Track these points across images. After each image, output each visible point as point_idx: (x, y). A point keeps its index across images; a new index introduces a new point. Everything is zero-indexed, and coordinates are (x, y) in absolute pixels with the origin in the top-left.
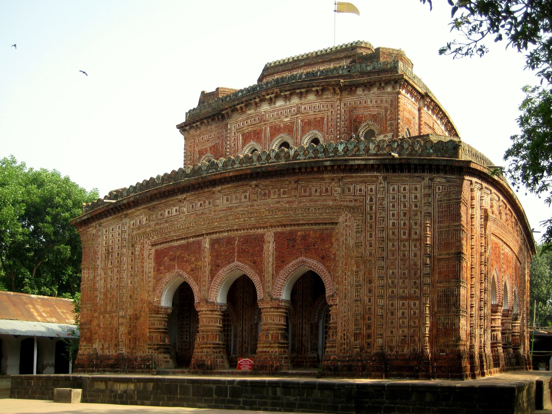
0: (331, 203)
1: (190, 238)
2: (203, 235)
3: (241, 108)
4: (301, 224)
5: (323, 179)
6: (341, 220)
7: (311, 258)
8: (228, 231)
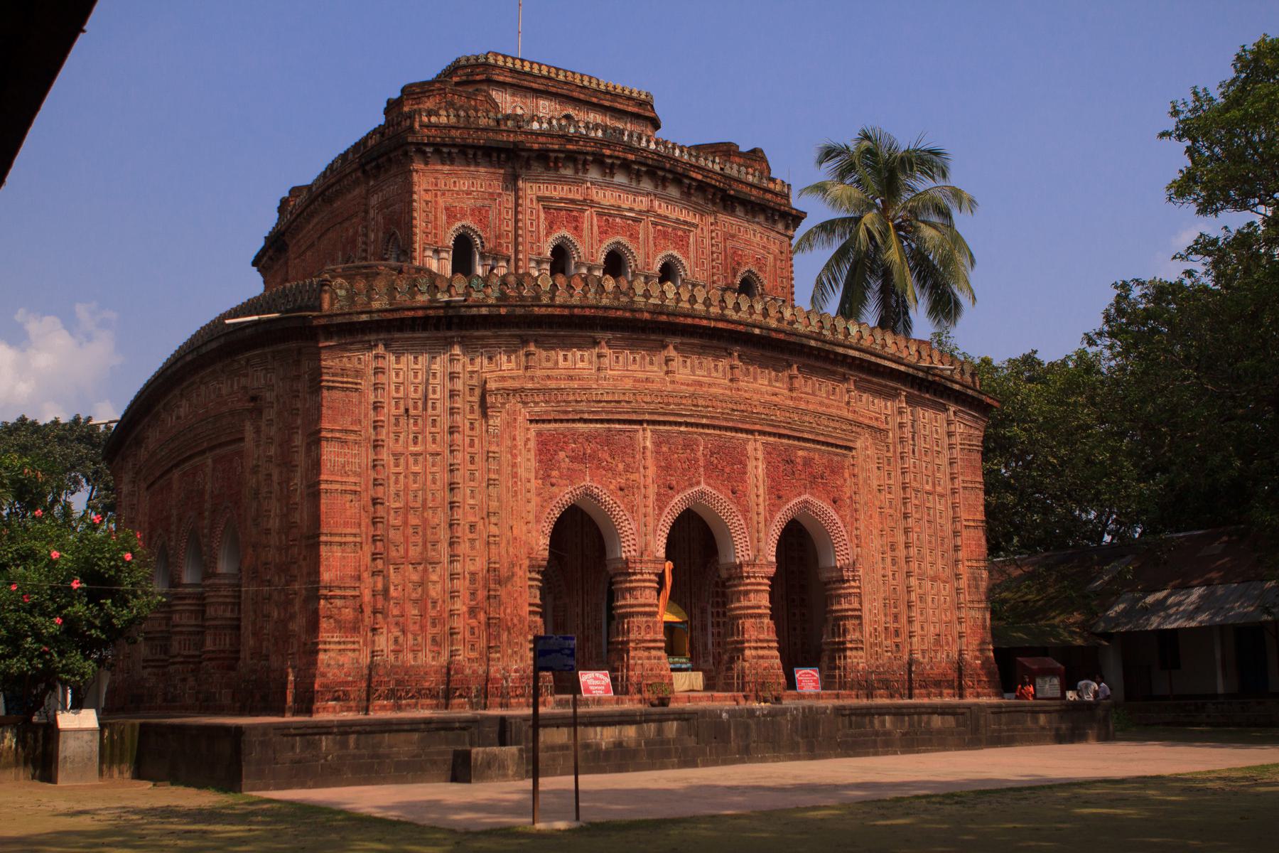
0: (850, 416)
2: (640, 422)
3: (556, 158)
5: (834, 373)
6: (859, 444)
7: (819, 498)
8: (687, 424)
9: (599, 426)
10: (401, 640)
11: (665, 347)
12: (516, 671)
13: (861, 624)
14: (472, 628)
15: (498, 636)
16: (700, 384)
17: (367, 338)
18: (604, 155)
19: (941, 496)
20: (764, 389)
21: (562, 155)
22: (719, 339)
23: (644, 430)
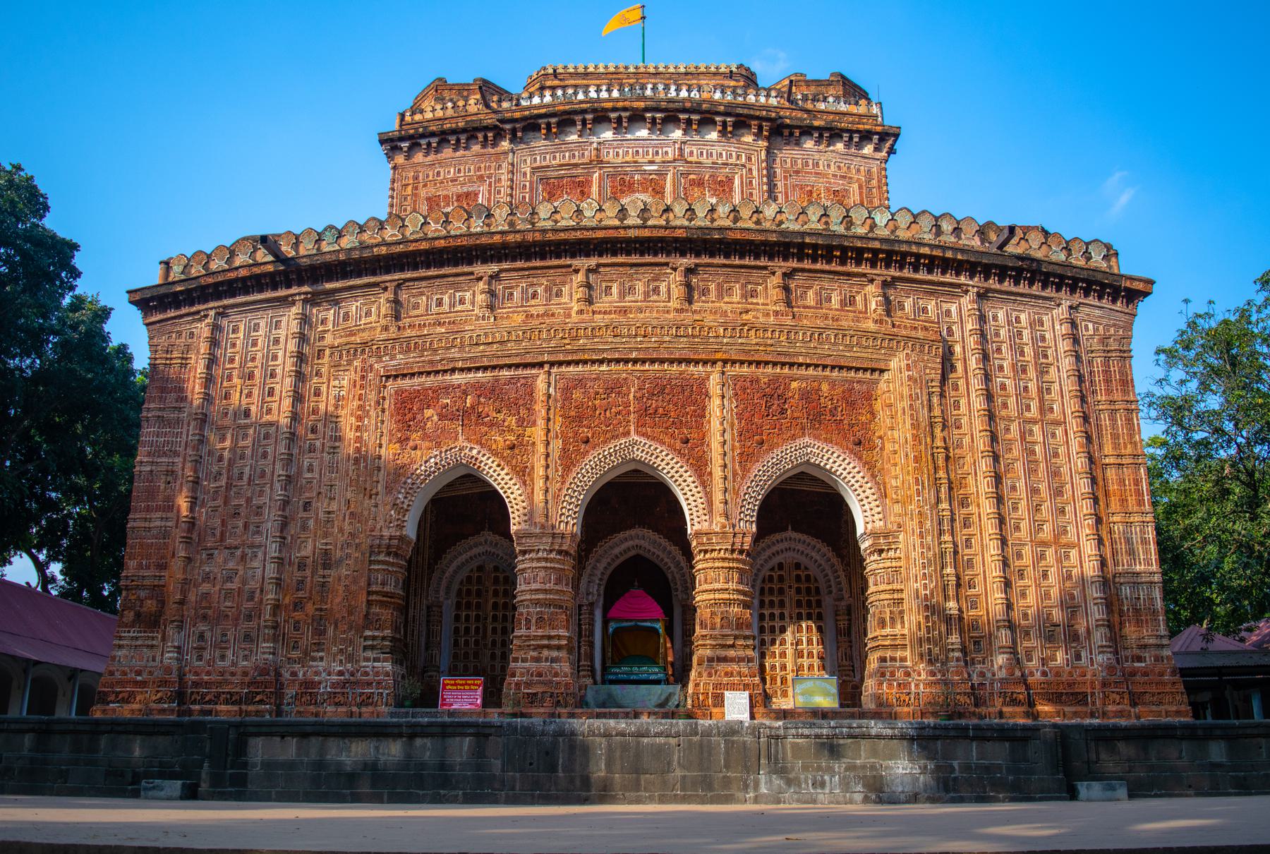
1: (501, 367)
2: (541, 365)
4: (800, 365)
6: (893, 364)
9: (480, 374)
10: (208, 635)
11: (577, 271)
12: (341, 673)
13: (902, 612)
14: (298, 622)
15: (322, 633)
16: (624, 311)
17: (194, 309)
18: (607, 110)
19: (1058, 423)
20: (728, 308)
21: (553, 120)
22: (655, 255)
23: (549, 373)
